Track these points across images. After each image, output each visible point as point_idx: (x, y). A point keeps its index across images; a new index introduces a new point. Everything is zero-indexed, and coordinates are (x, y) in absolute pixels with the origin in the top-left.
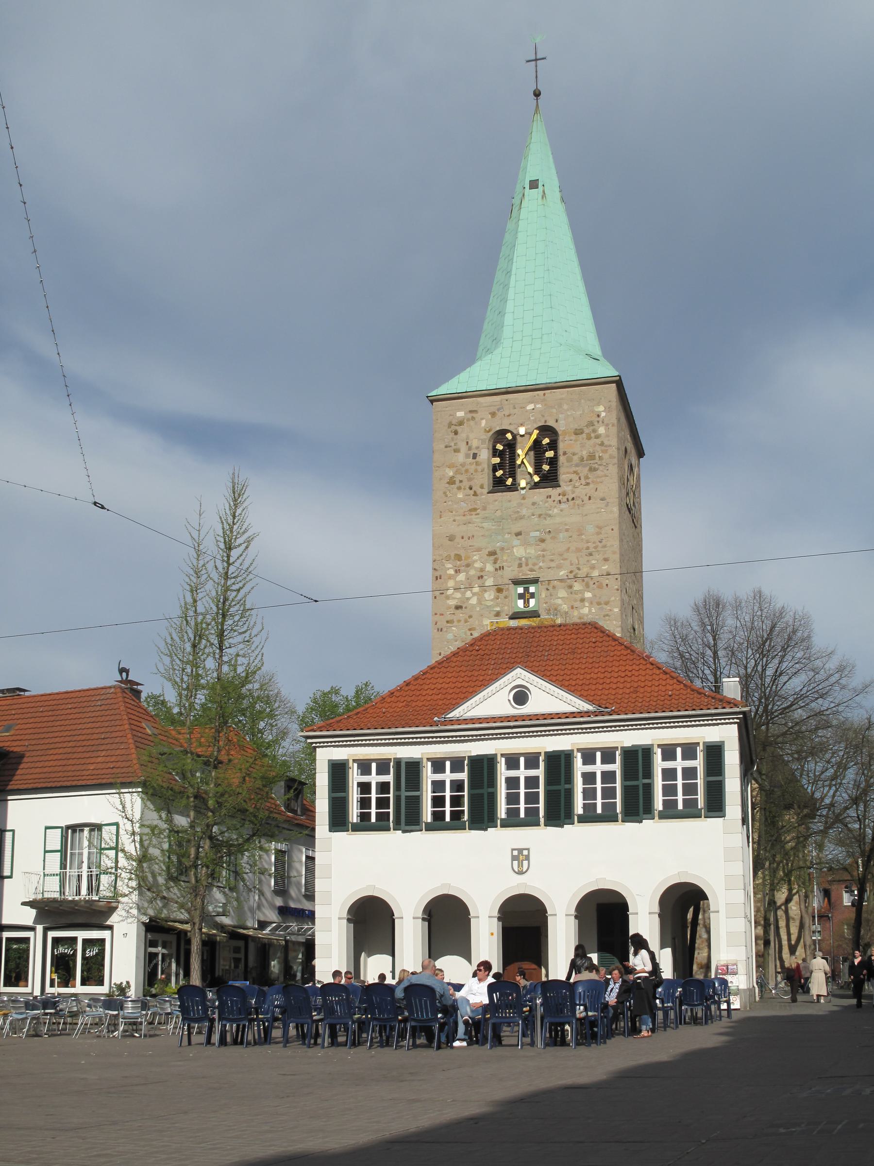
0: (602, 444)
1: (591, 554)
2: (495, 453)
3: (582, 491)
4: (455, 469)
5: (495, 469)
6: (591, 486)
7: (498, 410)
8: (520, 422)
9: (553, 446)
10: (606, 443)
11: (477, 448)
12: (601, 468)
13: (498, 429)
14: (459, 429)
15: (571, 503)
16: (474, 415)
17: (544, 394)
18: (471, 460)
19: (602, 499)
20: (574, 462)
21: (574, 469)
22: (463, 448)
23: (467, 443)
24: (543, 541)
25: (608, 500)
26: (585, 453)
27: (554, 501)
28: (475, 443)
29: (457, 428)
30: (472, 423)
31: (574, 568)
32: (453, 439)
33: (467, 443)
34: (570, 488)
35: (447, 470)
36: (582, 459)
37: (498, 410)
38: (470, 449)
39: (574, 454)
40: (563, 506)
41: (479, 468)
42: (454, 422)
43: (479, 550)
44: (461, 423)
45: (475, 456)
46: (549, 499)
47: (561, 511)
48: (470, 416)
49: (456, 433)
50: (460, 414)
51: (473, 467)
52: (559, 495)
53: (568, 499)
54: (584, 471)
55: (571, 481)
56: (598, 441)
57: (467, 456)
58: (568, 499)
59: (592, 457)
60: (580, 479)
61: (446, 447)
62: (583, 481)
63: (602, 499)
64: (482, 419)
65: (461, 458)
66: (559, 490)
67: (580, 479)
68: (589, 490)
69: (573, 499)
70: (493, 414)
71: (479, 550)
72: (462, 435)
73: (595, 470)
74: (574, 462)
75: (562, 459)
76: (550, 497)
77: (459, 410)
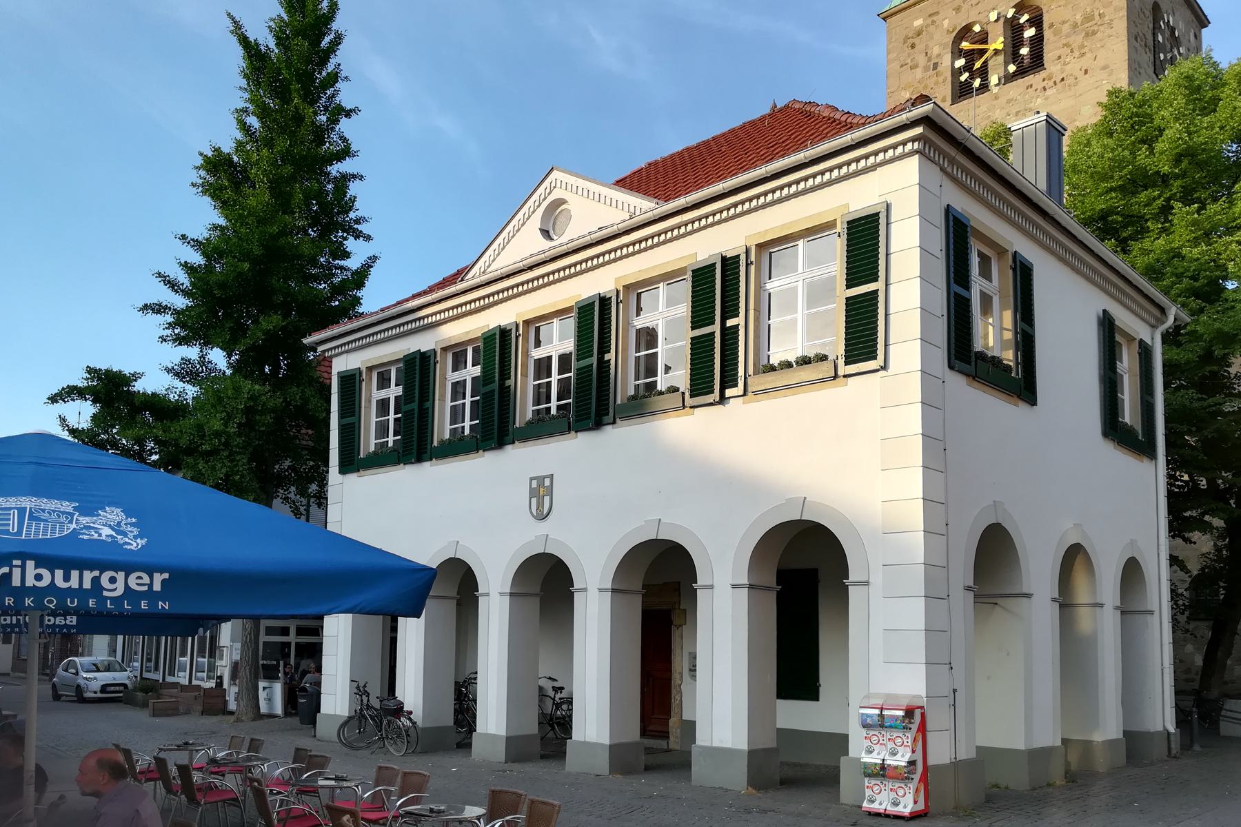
2: (957, 53)
3: (1075, 66)
4: (912, 89)
5: (956, 73)
6: (1089, 55)
8: (991, 7)
9: (1037, 22)
11: (939, 56)
12: (1102, 28)
14: (916, 41)
15: (1059, 85)
16: (935, 18)
18: (931, 72)
19: (1104, 68)
20: (1064, 33)
21: (1064, 42)
22: (922, 60)
23: (926, 53)
25: (1111, 68)
26: (1079, 18)
28: (936, 51)
29: (914, 40)
30: (932, 28)
32: (909, 55)
33: (926, 53)
34: (1059, 67)
35: (903, 93)
36: (1075, 25)
38: (929, 60)
39: (1064, 22)
40: (1049, 92)
41: (941, 79)
42: (910, 35)
44: (919, 33)
45: (935, 66)
46: (1029, 89)
47: (1046, 99)
48: (929, 21)
50: (918, 23)
51: (934, 79)
52: (1044, 80)
54: (1077, 40)
55: (1060, 57)
57: (926, 69)
58: (1055, 83)
59: (1088, 18)
60: (1072, 52)
61: (902, 66)
62: (1076, 54)
63: (1104, 68)
64: (944, 20)
66: (1043, 74)
67: (1072, 51)
68: (1086, 62)
69: (1063, 79)
70: (958, 9)
72: (920, 47)
73: (1094, 33)
74: (1064, 33)
76: (1031, 86)
77: (917, 18)
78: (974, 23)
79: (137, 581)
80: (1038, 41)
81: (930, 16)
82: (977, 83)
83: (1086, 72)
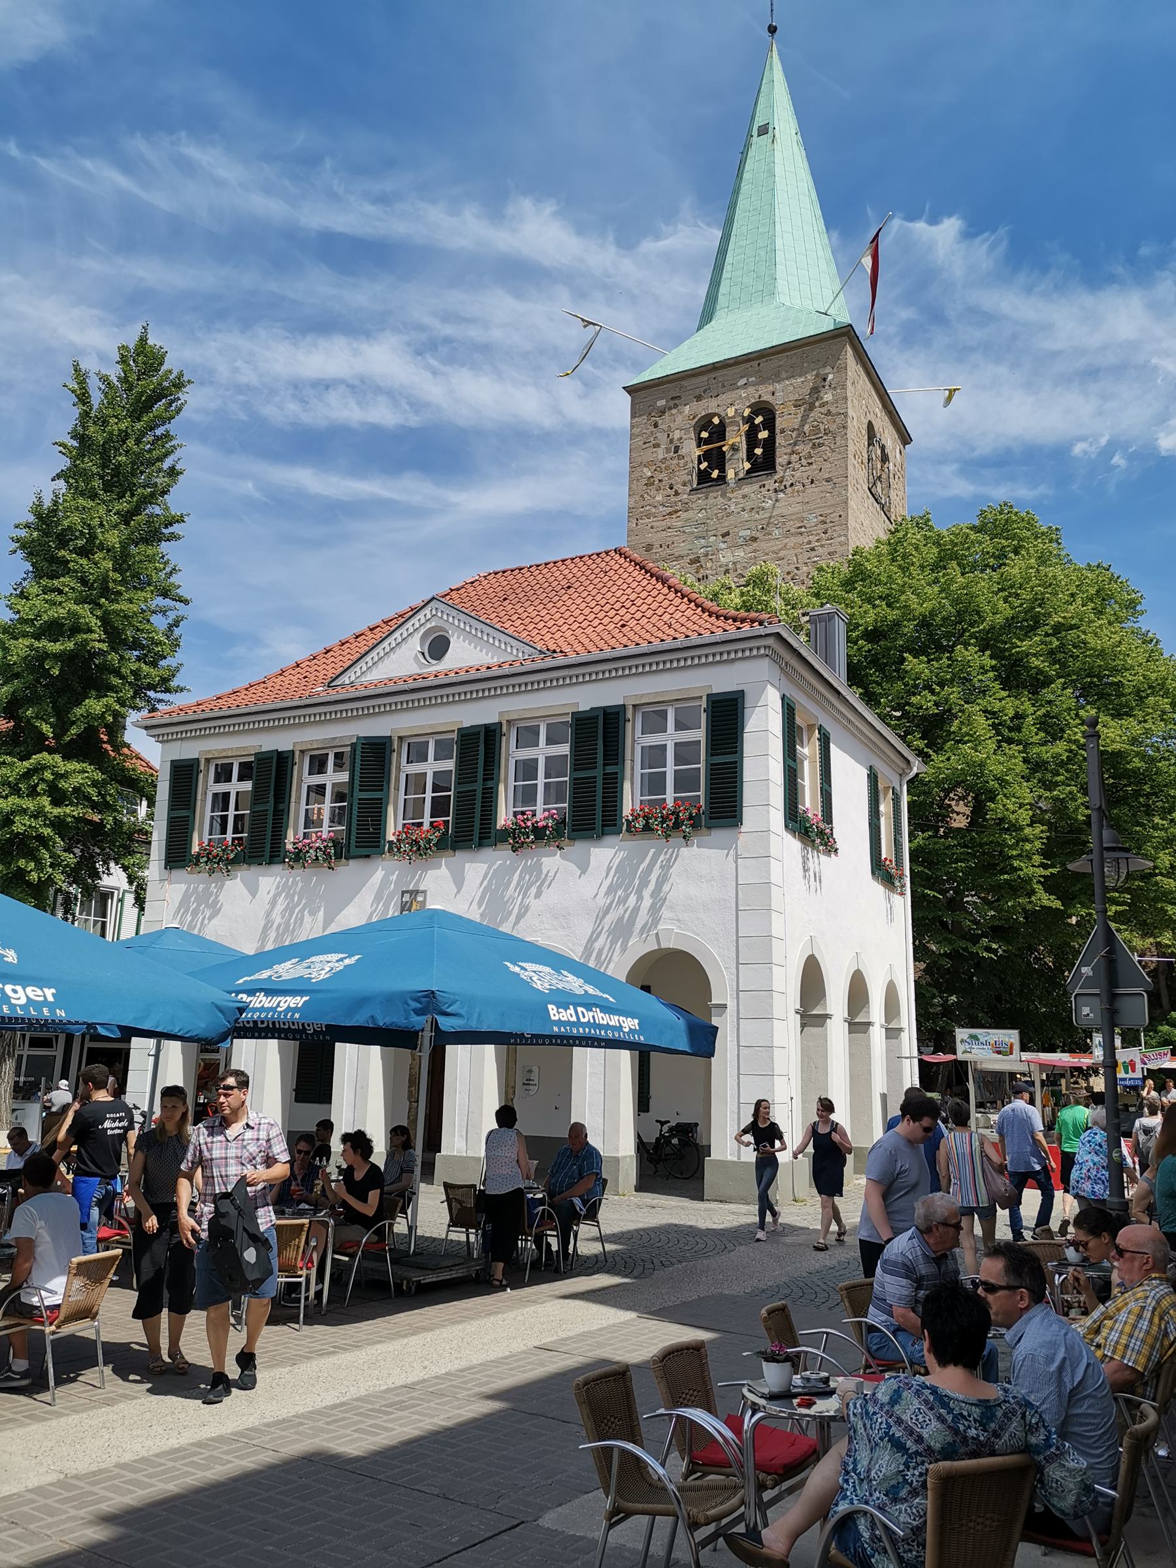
0: (829, 413)
1: (813, 549)
7: (704, 392)
8: (730, 401)
9: (770, 424)
10: (834, 410)
13: (703, 413)
16: (677, 402)
17: (759, 364)
22: (662, 438)
24: (754, 539)
27: (769, 490)
28: (677, 435)
31: (791, 568)
35: (645, 470)
37: (704, 392)
38: (671, 441)
43: (678, 558)
48: (671, 403)
49: (656, 425)
50: (661, 403)
53: (785, 486)
56: (824, 410)
57: (668, 450)
58: (785, 486)
65: (661, 453)
68: (812, 471)
69: (792, 485)
71: (678, 558)
73: (820, 445)
75: (779, 440)
78: (714, 415)
79: (33, 992)
80: (770, 444)
81: (672, 398)
82: (715, 474)
83: (812, 482)
